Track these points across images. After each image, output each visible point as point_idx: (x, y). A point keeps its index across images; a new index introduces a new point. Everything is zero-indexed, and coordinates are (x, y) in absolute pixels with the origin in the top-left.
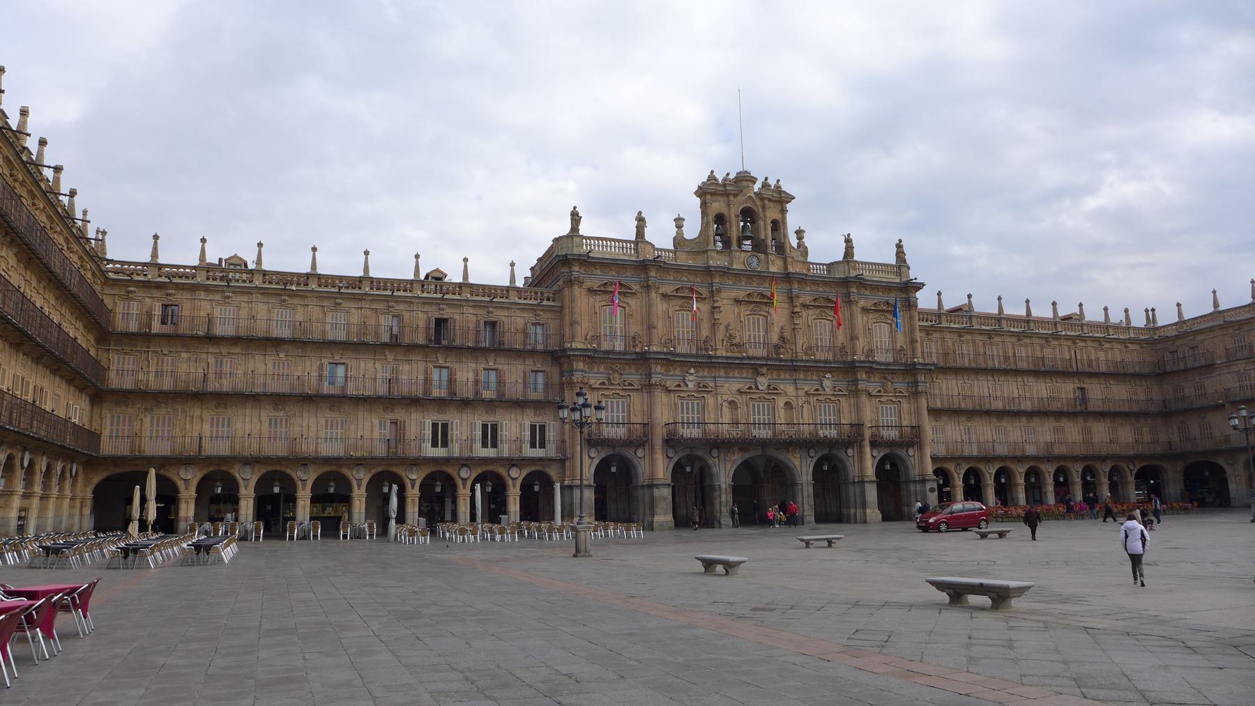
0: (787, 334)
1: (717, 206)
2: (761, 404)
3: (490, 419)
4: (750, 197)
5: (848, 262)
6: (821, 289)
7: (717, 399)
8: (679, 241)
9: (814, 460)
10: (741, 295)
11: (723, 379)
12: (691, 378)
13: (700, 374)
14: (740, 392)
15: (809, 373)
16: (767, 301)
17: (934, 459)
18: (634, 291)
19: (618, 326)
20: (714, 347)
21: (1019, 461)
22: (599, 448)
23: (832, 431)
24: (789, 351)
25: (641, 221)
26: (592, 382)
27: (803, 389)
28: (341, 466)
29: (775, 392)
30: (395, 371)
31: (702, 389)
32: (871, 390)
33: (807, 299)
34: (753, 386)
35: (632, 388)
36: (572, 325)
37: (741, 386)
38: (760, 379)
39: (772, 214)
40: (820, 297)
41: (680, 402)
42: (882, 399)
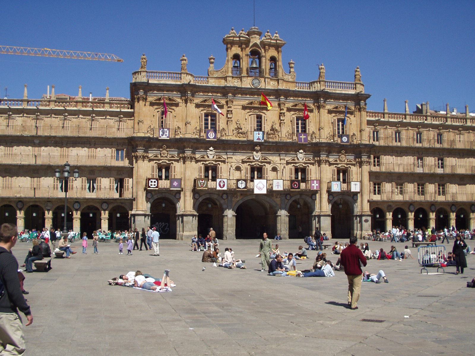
0: (277, 127)
5: (320, 82)
7: (228, 165)
9: (290, 202)
10: (245, 103)
12: (211, 152)
17: (371, 202)
20: (227, 134)
24: (277, 135)
26: (150, 155)
29: (265, 161)
34: (252, 158)
36: (138, 123)
37: (244, 157)
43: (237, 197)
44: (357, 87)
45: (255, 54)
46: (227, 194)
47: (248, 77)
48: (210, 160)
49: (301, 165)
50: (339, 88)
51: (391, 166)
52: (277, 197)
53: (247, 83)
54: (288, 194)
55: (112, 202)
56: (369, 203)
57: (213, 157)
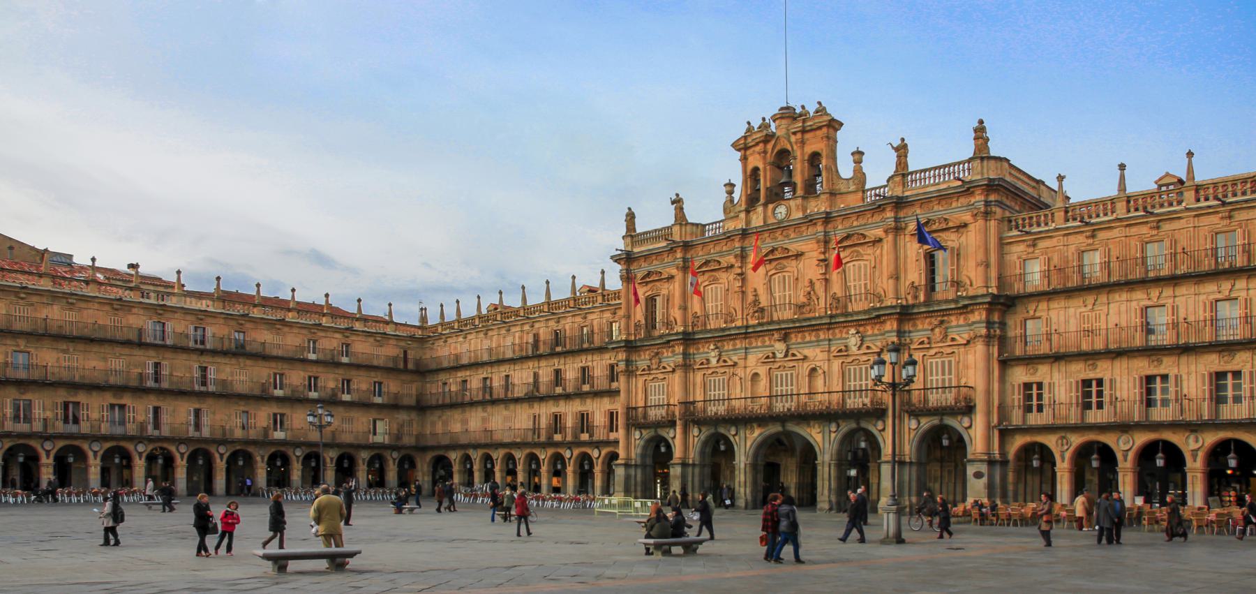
1: (755, 161)
3: (554, 409)
6: (855, 224)
8: (729, 206)
9: (840, 436)
12: (713, 354)
13: (726, 348)
15: (837, 331)
21: (1192, 431)
22: (643, 431)
23: (719, 408)
25: (677, 202)
28: (511, 449)
30: (536, 376)
40: (853, 234)
42: (932, 352)
43: (753, 432)
45: (783, 155)
57: (718, 361)
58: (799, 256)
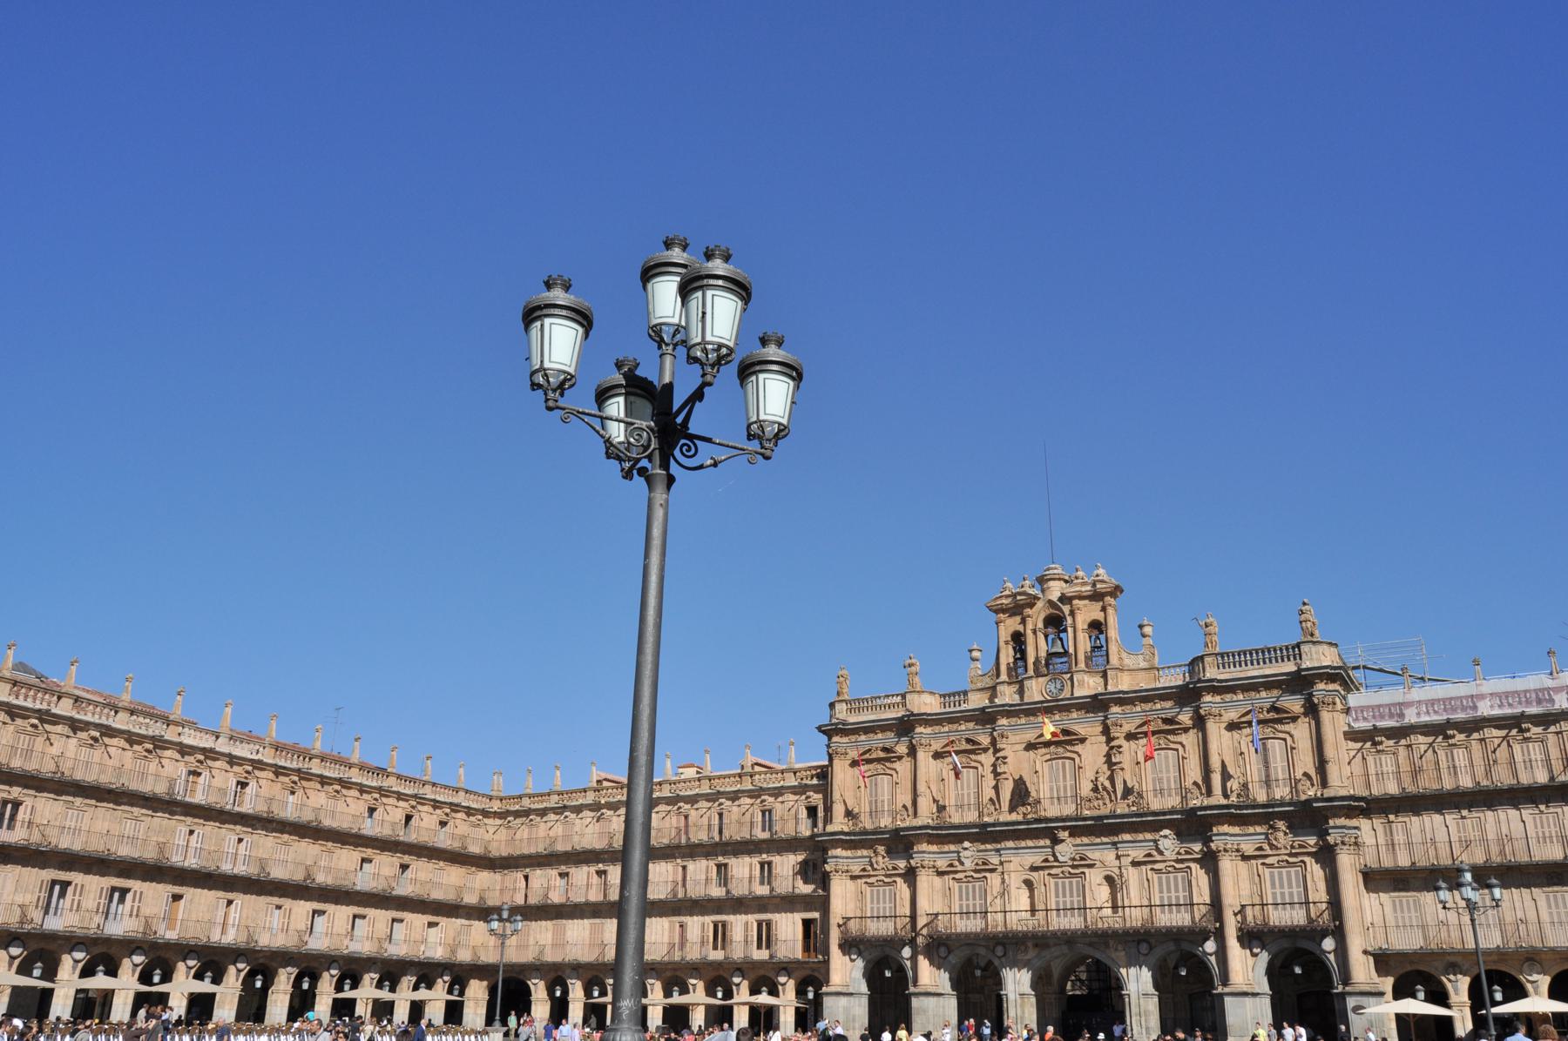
2: (1067, 880)
4: (1050, 602)
10: (1031, 736)
11: (1013, 851)
12: (966, 853)
14: (1034, 869)
16: (1068, 739)
18: (898, 754)
19: (886, 798)
27: (1128, 855)
31: (984, 868)
32: (1243, 847)
33: (1129, 727)
34: (1051, 858)
35: (896, 872)
38: (1058, 848)
39: (1087, 612)
41: (957, 885)
42: (1269, 861)
43: (1026, 951)
44: (1302, 650)
45: (1055, 622)
46: (1004, 945)
47: (1037, 677)
48: (965, 871)
49: (1170, 866)
50: (1232, 666)
51: (1520, 846)
52: (1116, 950)
53: (1036, 690)
54: (1145, 941)
55: (797, 968)
56: (1371, 959)
58: (1083, 740)
